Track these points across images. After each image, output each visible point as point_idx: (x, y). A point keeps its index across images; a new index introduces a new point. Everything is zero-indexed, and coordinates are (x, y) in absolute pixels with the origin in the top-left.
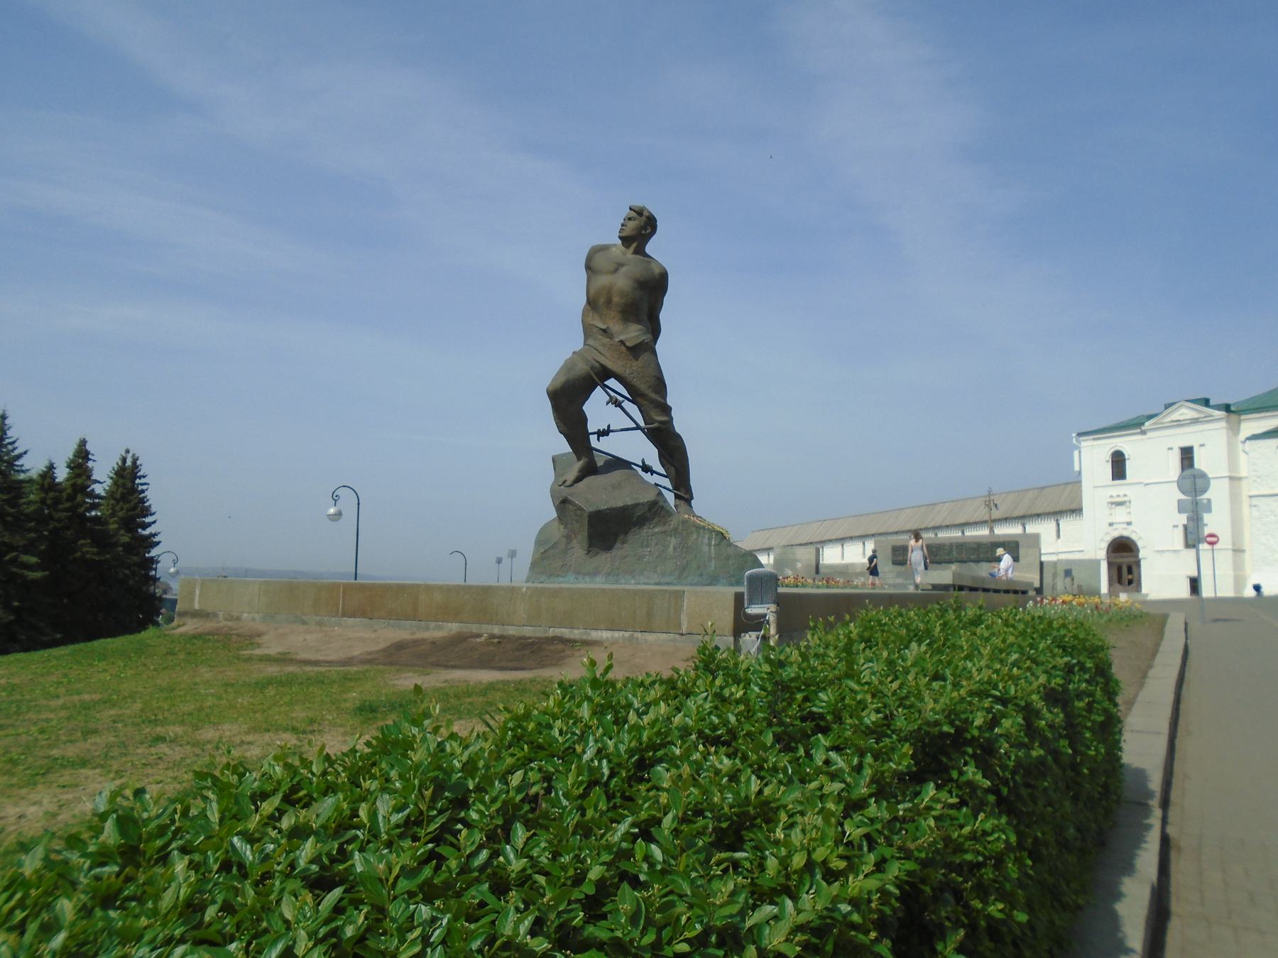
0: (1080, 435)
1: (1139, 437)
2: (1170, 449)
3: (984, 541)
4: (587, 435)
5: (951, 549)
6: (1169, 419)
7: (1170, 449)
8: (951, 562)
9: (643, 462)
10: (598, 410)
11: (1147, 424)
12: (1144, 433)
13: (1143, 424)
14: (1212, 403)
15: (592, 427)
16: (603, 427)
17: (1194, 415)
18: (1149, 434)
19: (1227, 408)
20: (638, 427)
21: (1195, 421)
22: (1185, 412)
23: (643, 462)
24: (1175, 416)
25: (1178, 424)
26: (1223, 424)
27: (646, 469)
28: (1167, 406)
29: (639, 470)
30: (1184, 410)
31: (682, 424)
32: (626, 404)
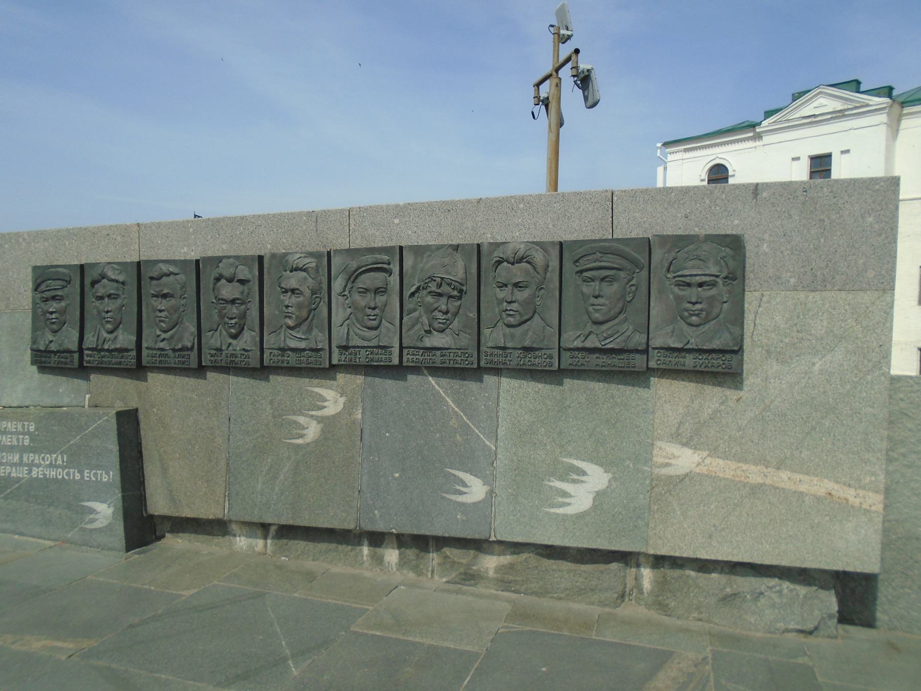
0: (666, 144)
1: (751, 144)
2: (798, 159)
3: (516, 234)
5: (323, 293)
6: (797, 116)
7: (798, 159)
8: (329, 371)
11: (765, 123)
12: (758, 137)
13: (760, 124)
14: (862, 89)
17: (838, 105)
18: (767, 139)
19: (888, 91)
21: (839, 115)
22: (824, 103)
24: (808, 110)
25: (814, 120)
26: (883, 118)
28: (796, 97)
30: (822, 101)
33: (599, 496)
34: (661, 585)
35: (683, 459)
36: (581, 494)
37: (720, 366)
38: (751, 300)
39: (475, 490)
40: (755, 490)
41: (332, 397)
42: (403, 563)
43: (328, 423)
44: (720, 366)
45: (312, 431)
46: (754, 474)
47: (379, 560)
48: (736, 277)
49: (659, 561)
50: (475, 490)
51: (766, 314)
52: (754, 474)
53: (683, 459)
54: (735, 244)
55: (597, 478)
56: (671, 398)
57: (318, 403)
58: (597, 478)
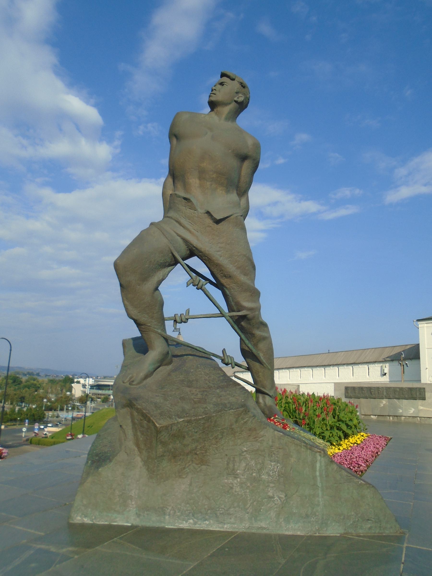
0: (418, 320)
4: (162, 320)
9: (224, 351)
10: (177, 290)
15: (168, 312)
16: (180, 311)
20: (222, 315)
23: (224, 351)
27: (227, 361)
29: (219, 361)
31: (270, 311)
32: (209, 287)
33: (414, 411)
34: (420, 419)
35: (421, 408)
36: (412, 411)
37: (424, 399)
38: (426, 394)
39: (401, 411)
40: (428, 410)
41: (384, 401)
42: (393, 419)
43: (384, 404)
44: (424, 399)
45: (382, 405)
46: (428, 409)
47: (390, 419)
48: (425, 392)
49: (420, 417)
50: (401, 411)
51: (427, 395)
52: (428, 409)
53: (421, 408)
54: (424, 388)
55: (413, 410)
56: (420, 402)
57: (383, 402)
58: (413, 410)
